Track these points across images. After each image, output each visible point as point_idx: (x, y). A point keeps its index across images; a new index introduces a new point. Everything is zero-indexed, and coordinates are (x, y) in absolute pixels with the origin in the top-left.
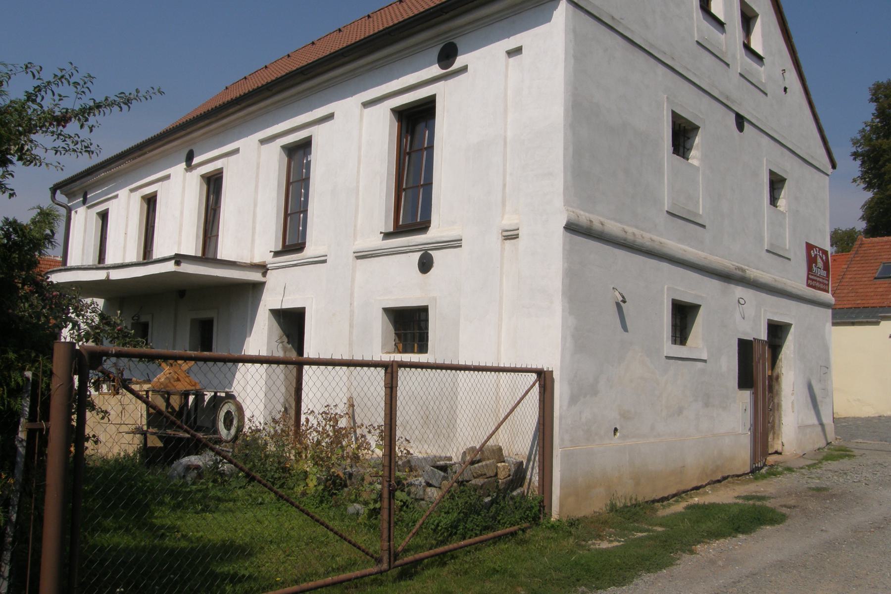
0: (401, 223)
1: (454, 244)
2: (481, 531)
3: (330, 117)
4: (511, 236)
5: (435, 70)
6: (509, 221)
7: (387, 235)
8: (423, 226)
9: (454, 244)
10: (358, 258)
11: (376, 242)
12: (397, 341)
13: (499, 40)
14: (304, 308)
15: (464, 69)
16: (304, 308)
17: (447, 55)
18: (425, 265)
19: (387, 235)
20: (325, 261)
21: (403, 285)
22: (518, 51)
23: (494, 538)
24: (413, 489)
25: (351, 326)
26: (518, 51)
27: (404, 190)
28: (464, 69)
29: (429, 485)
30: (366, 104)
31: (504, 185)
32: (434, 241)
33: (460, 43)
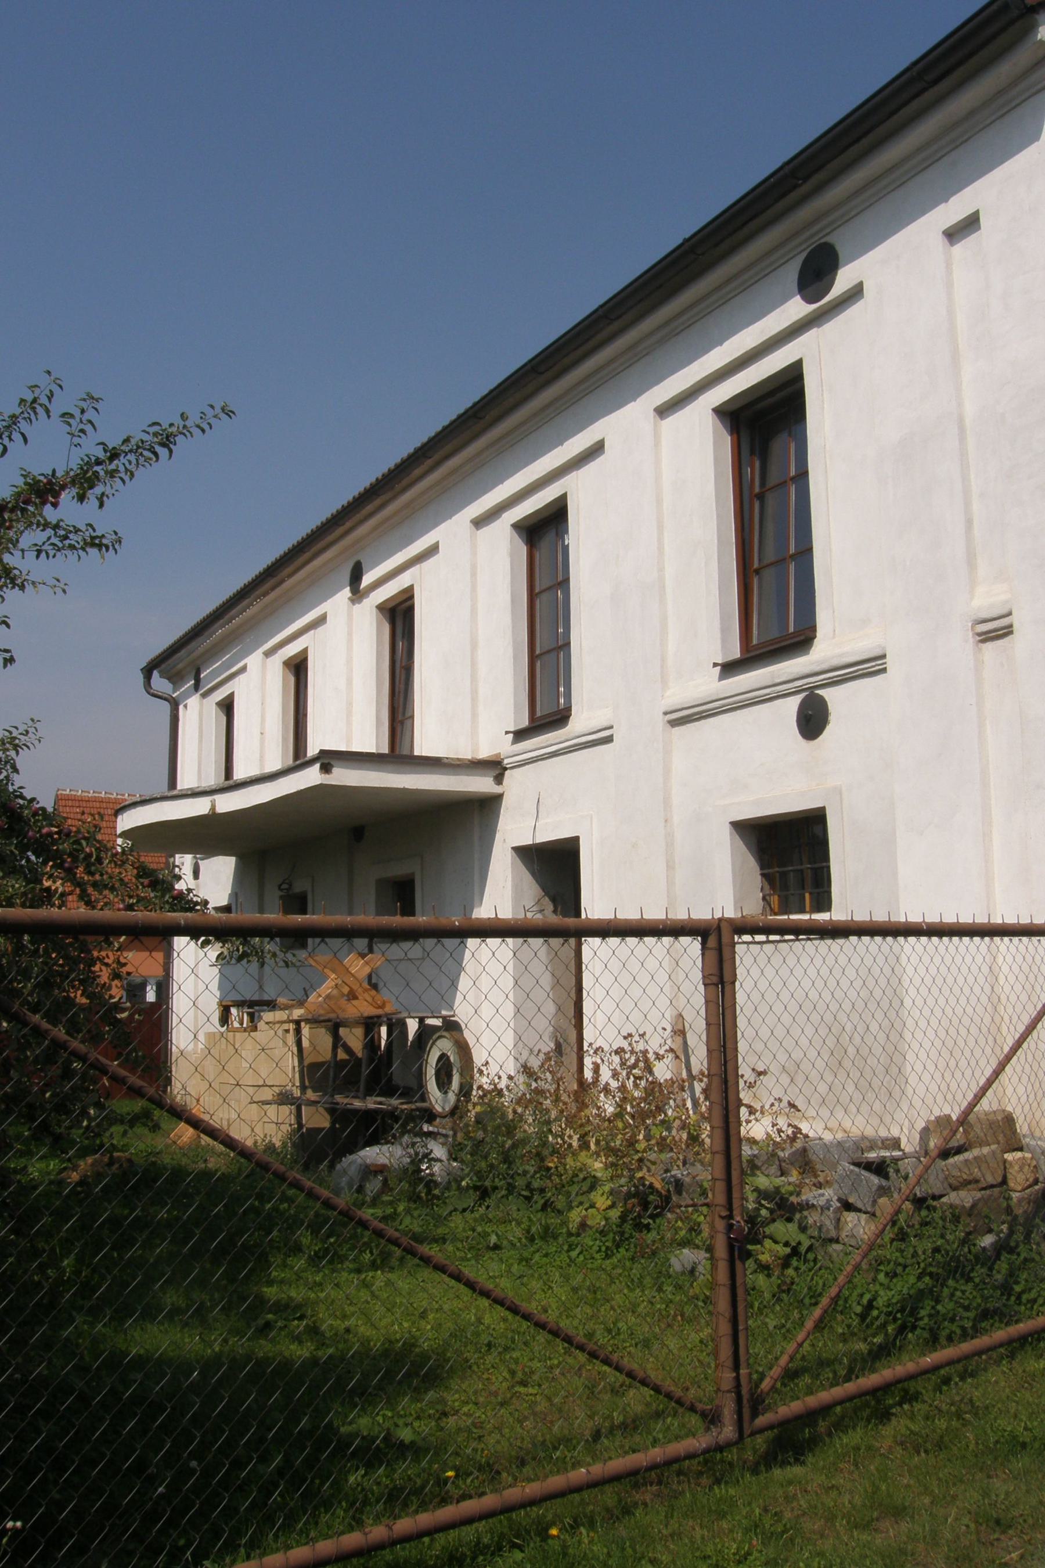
0: (755, 642)
1: (871, 666)
2: (976, 1321)
3: (597, 449)
4: (995, 631)
5: (796, 308)
6: (987, 599)
7: (729, 669)
8: (802, 640)
9: (871, 666)
10: (674, 723)
11: (707, 685)
12: (767, 887)
13: (923, 212)
14: (576, 840)
15: (856, 293)
16: (576, 840)
17: (817, 272)
18: (812, 720)
19: (729, 669)
20: (609, 740)
21: (767, 767)
22: (971, 224)
23: (1010, 1342)
24: (812, 1218)
25: (670, 866)
26: (971, 224)
27: (757, 572)
28: (856, 293)
29: (848, 1207)
30: (664, 410)
31: (969, 522)
32: (825, 666)
33: (840, 240)
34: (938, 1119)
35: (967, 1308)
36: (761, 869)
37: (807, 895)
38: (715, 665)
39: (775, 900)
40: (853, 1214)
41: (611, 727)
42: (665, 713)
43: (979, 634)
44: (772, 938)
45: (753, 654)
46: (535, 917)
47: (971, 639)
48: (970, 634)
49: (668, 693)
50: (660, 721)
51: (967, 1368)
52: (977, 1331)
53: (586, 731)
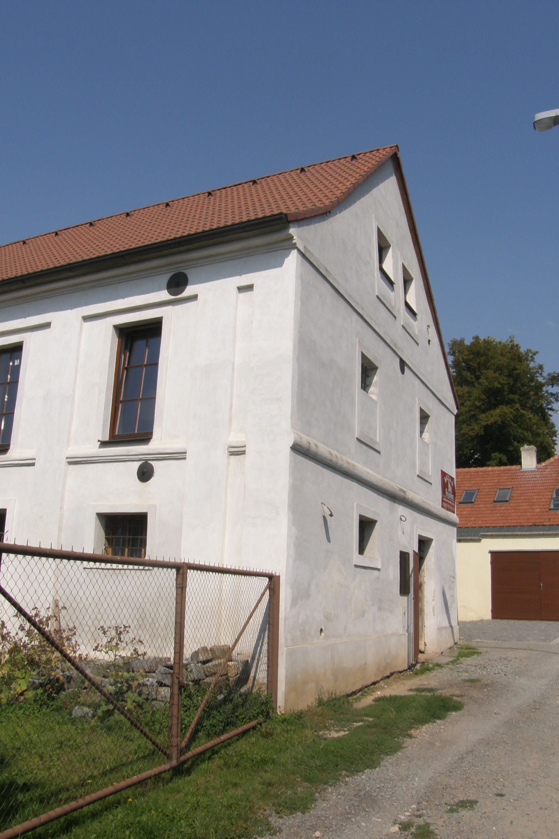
0: (116, 433)
1: (180, 456)
2: (224, 727)
3: (47, 325)
4: (237, 452)
5: (164, 295)
6: (236, 439)
7: (104, 444)
8: (145, 437)
9: (180, 456)
10: (70, 463)
11: (93, 449)
12: (107, 544)
13: (230, 276)
15: (194, 298)
17: (177, 283)
18: (145, 474)
19: (104, 444)
20: (33, 464)
21: (121, 492)
22: (250, 288)
23: (237, 735)
24: (145, 690)
25: (60, 529)
26: (250, 288)
27: (121, 402)
28: (194, 298)
29: (161, 684)
30: (86, 319)
31: (231, 406)
33: (190, 274)
34: (203, 648)
35: (221, 722)
36: (106, 535)
37: (126, 550)
38: (99, 441)
39: (110, 550)
40: (164, 688)
41: (35, 459)
42: (67, 458)
43: (230, 452)
44: (147, 568)
45: (114, 440)
46: (100, 552)
47: (227, 453)
48: (227, 451)
49: (69, 449)
50: (65, 461)
51: (227, 744)
52: (222, 732)
53: (18, 458)
